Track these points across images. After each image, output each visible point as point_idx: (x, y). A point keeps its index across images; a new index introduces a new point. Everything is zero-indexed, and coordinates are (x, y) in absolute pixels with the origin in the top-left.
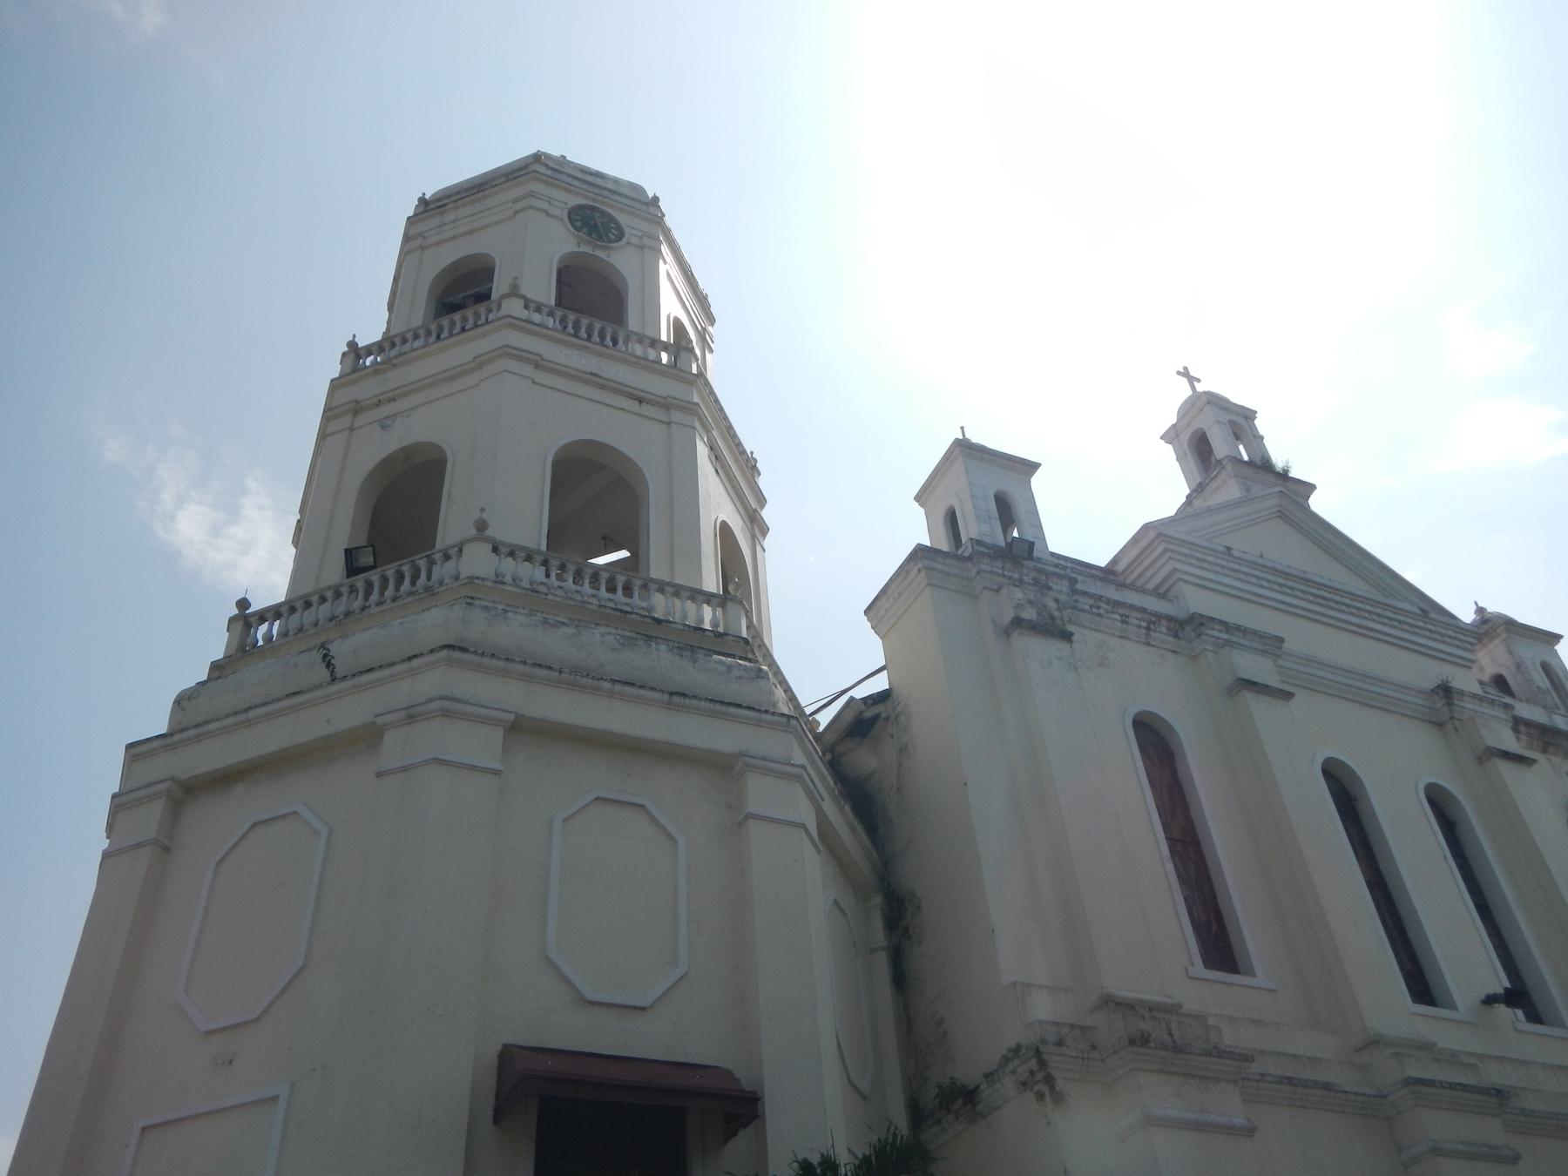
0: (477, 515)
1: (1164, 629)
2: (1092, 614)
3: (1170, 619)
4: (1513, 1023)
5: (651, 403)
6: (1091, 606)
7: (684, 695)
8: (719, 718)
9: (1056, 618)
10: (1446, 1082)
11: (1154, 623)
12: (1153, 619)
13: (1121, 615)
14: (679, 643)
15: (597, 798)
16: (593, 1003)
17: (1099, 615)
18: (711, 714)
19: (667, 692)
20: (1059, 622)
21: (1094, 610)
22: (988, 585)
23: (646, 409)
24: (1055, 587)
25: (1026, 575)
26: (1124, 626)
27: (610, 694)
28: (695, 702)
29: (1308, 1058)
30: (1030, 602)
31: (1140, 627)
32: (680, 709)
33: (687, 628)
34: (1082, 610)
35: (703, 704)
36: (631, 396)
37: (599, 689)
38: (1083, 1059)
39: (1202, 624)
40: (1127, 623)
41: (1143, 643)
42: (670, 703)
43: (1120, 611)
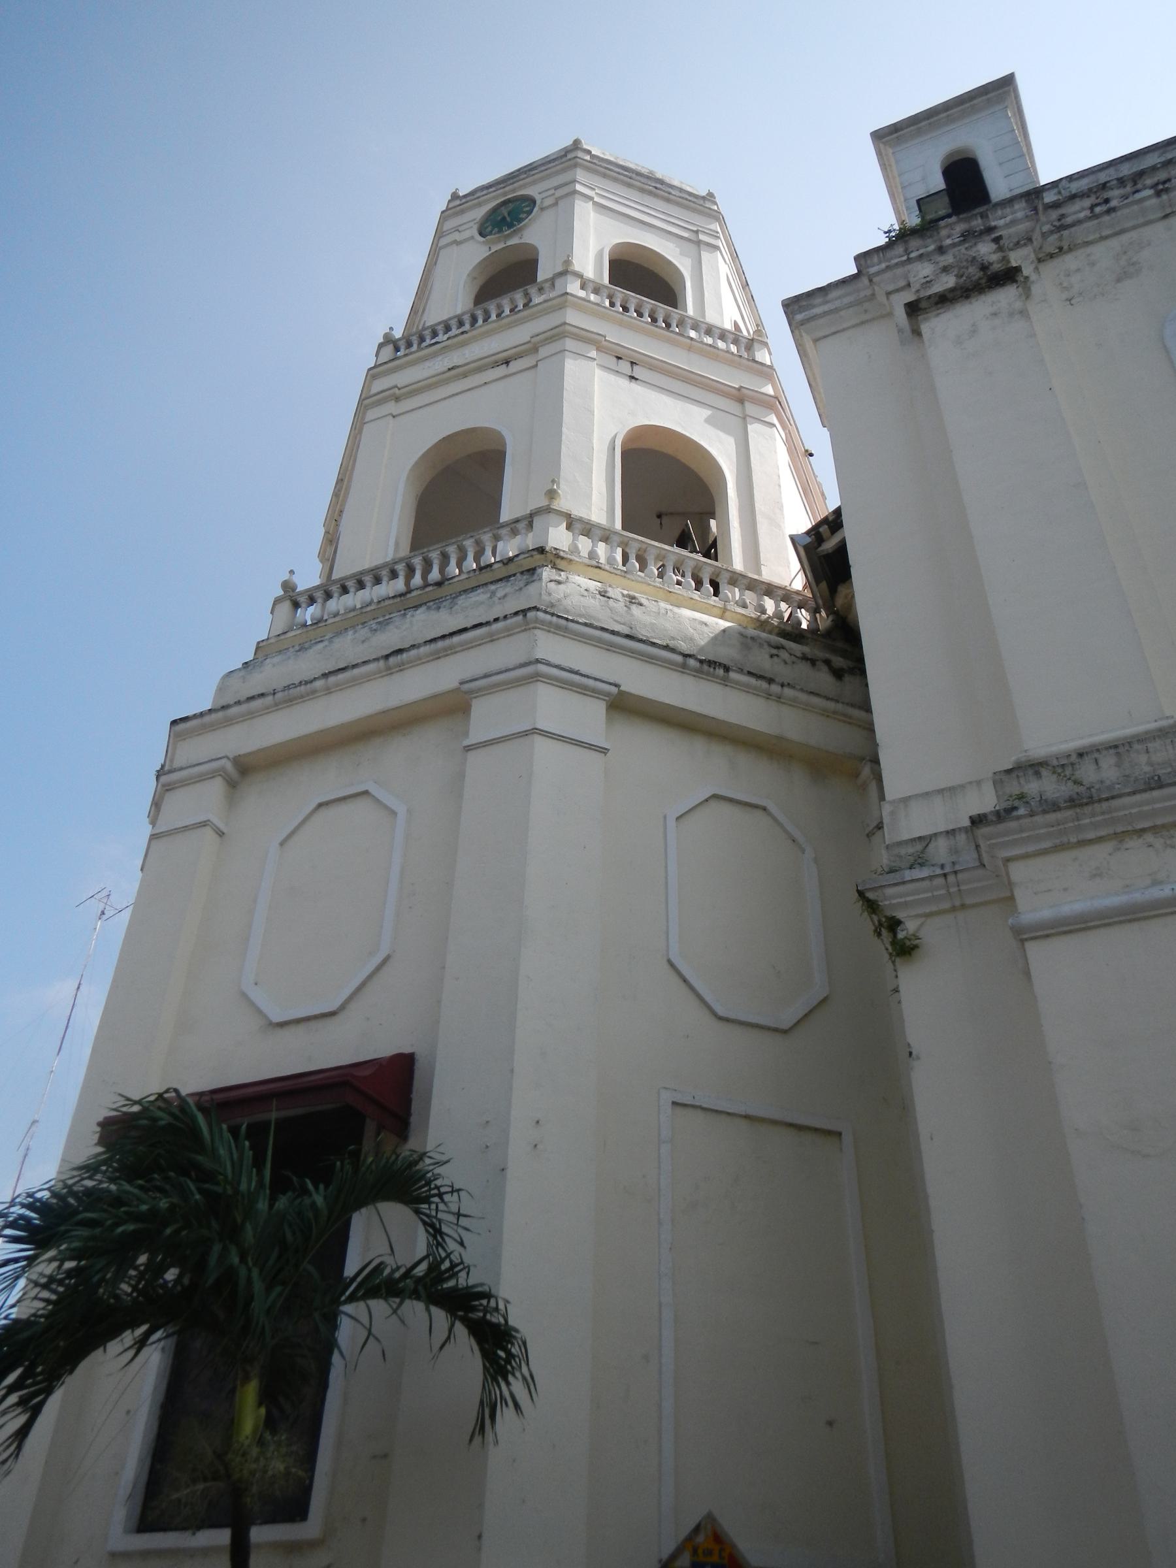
0: (286, 577)
2: (1096, 217)
5: (519, 356)
6: (1092, 208)
7: (400, 651)
8: (447, 655)
9: (991, 264)
13: (1154, 186)
14: (451, 595)
15: (320, 805)
16: (282, 1025)
17: (1110, 211)
18: (437, 656)
19: (382, 657)
20: (1000, 265)
21: (1098, 210)
22: (891, 288)
23: (515, 366)
24: (1001, 222)
25: (949, 237)
26: (1165, 197)
27: (328, 691)
28: (413, 652)
30: (945, 269)
32: (402, 667)
33: (472, 574)
34: (1080, 222)
35: (423, 650)
36: (496, 364)
37: (314, 692)
38: (945, 875)
40: (1167, 190)
42: (389, 668)
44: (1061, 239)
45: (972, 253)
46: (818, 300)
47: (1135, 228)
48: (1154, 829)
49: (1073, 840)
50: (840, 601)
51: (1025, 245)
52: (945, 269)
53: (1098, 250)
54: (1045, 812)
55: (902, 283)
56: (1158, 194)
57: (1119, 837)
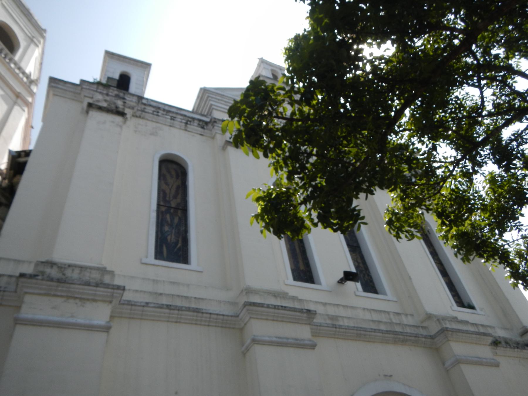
1: (196, 124)
2: (153, 114)
3: (200, 120)
4: (355, 292)
10: (272, 305)
11: (190, 121)
12: (190, 119)
13: (171, 117)
17: (158, 115)
21: (155, 113)
22: (87, 95)
24: (128, 99)
26: (172, 121)
29: (195, 298)
31: (181, 122)
39: (215, 122)
40: (174, 120)
41: (182, 129)
43: (171, 114)
44: (141, 114)
45: (116, 101)
46: (62, 83)
47: (162, 124)
48: (81, 299)
49: (52, 293)
50: (15, 180)
51: (131, 109)
52: (106, 101)
53: (149, 123)
54: (48, 280)
55: (91, 96)
56: (171, 119)
57: (68, 297)
